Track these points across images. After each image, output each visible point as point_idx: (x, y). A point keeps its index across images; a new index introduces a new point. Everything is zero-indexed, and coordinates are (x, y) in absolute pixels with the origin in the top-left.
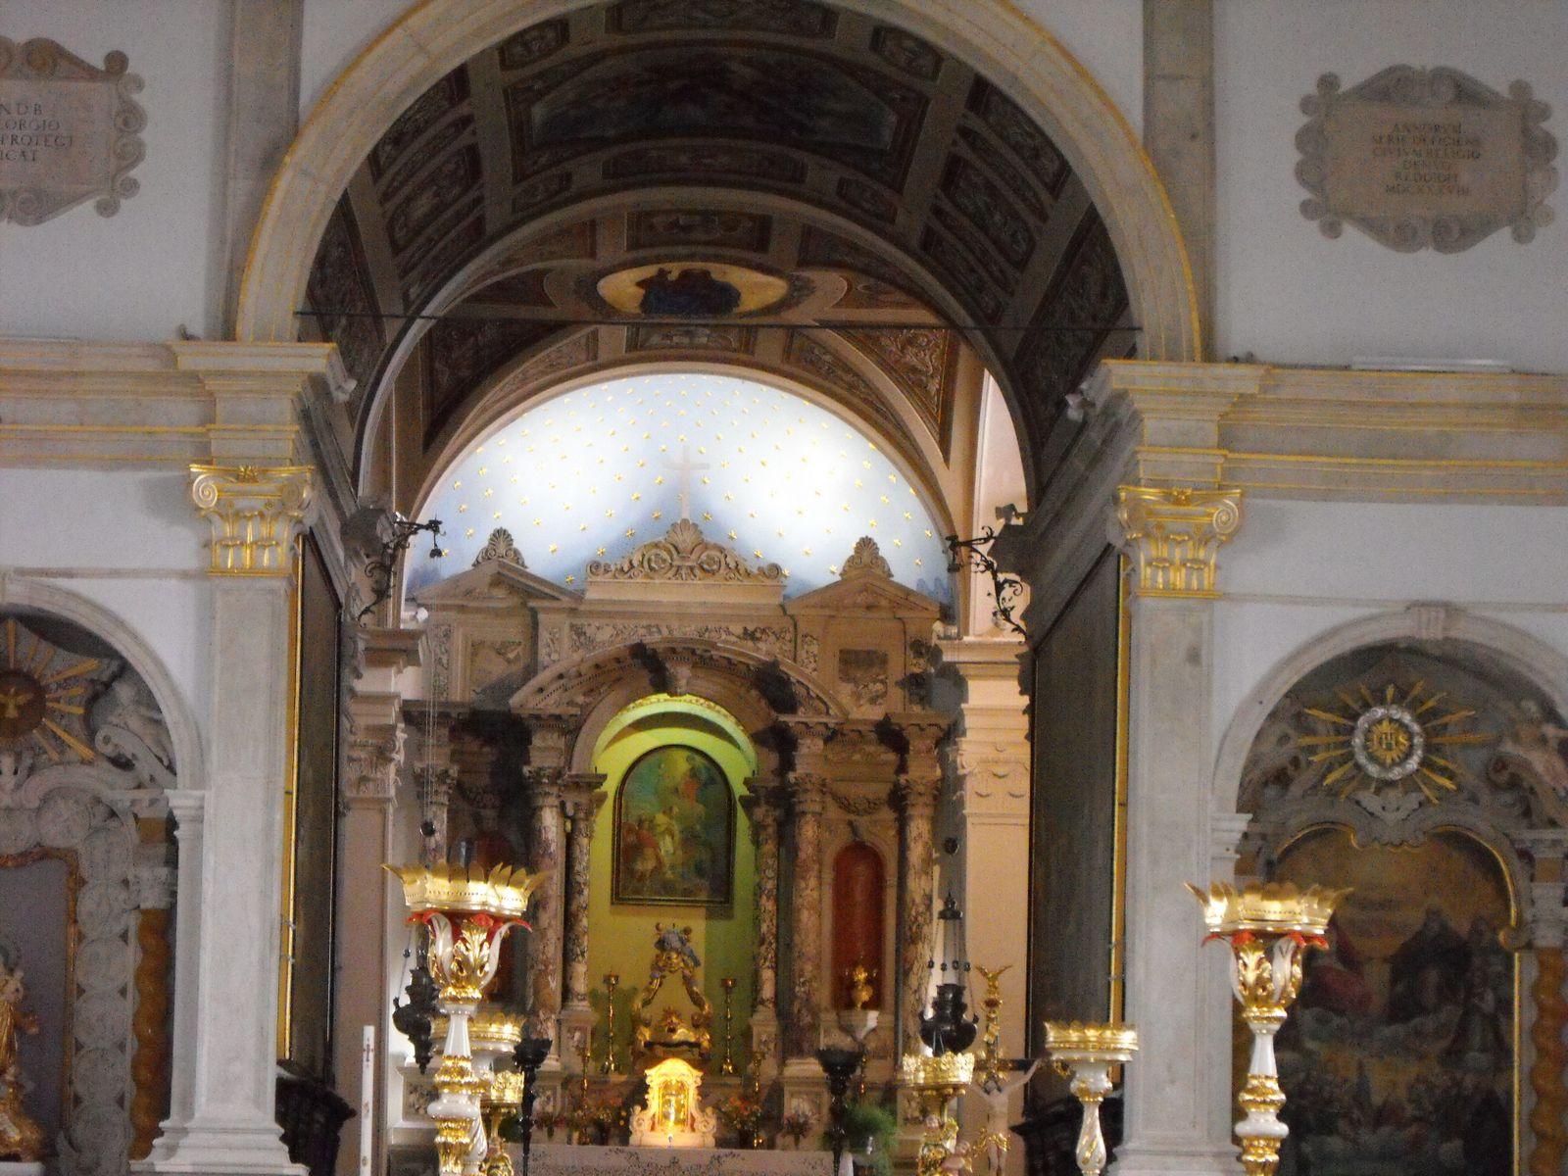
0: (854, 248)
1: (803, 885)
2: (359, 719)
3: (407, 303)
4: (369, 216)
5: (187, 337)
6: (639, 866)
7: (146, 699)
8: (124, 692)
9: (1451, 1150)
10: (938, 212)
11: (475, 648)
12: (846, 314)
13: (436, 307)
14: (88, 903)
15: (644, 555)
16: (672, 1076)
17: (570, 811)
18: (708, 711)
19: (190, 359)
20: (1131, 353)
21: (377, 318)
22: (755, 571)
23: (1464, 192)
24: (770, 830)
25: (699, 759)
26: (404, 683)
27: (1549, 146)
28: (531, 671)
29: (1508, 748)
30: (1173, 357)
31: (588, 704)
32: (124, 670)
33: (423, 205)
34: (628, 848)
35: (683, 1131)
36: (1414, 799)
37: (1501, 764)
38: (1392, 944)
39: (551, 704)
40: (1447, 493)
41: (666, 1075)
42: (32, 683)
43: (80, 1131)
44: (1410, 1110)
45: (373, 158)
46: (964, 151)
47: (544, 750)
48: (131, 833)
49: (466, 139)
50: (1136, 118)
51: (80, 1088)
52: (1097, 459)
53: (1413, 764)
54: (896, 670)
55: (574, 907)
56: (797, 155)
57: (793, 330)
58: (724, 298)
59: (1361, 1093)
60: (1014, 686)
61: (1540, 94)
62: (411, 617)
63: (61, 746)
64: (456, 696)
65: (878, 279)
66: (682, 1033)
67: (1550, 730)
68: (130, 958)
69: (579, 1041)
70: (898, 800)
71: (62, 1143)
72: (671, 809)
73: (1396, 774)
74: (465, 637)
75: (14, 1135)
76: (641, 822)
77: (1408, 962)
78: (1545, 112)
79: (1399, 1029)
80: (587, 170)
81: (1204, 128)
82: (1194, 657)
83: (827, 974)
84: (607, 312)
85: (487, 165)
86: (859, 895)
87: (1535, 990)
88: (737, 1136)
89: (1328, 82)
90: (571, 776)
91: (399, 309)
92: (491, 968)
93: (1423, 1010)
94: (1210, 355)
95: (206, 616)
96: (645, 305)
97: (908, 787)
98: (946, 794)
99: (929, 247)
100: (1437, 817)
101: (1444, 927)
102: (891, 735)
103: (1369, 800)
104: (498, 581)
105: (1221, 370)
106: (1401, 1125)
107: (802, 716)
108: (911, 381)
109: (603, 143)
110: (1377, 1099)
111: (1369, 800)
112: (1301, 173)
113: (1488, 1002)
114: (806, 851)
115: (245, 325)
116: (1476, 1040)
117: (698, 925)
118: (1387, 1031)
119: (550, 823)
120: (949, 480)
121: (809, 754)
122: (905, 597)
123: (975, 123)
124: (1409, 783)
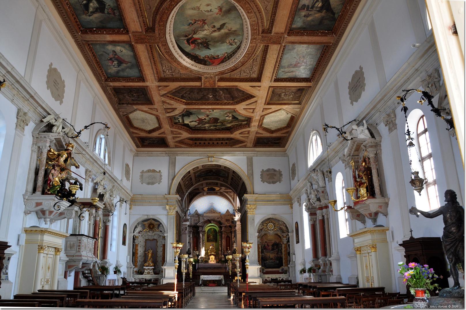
0: (225, 185)
2: (183, 227)
3: (186, 191)
4: (182, 183)
5: (166, 195)
7: (163, 226)
8: (161, 225)
9: (278, 262)
10: (231, 182)
11: (194, 220)
12: (225, 190)
13: (189, 191)
14: (158, 243)
16: (212, 257)
19: (166, 196)
20: (247, 194)
21: (184, 192)
23: (275, 179)
26: (188, 223)
27: (282, 175)
28: (199, 222)
29: (281, 226)
30: (250, 194)
32: (161, 223)
33: (187, 183)
34: (208, 237)
36: (273, 231)
37: (280, 228)
38: (272, 244)
39: (201, 225)
40: (275, 205)
42: (153, 224)
43: (157, 264)
44: (274, 258)
45: (182, 178)
46: (233, 177)
47: (200, 229)
48: (162, 237)
49: (190, 177)
50: (247, 174)
51: (157, 260)
52: (245, 203)
53: (273, 228)
54: (231, 221)
56: (219, 177)
57: (220, 192)
58: (214, 190)
59: (269, 257)
60: (239, 222)
61: (281, 170)
62: (189, 218)
63: (156, 230)
64: (193, 224)
65: (228, 188)
66: (213, 253)
67: (284, 225)
68: (162, 248)
70: (231, 232)
71: (156, 265)
73: (271, 229)
75: (151, 264)
77: (273, 245)
78: (281, 172)
79: (273, 251)
80: (201, 179)
81: (252, 175)
82: (253, 220)
83: (225, 248)
84: (205, 191)
85: (192, 179)
86: (228, 240)
87: (284, 247)
88: (217, 262)
89: (263, 170)
91: (185, 191)
92: (179, 252)
93: (274, 250)
94: (254, 194)
95: (168, 218)
96: (208, 190)
98: (235, 231)
99: (231, 185)
100: (275, 233)
101: (276, 242)
102: (230, 226)
103: (269, 231)
104: (196, 214)
105: (255, 195)
106: (273, 260)
107: (223, 225)
108: (231, 196)
109: (203, 177)
110: (271, 257)
111: (269, 231)
112: (261, 178)
113: (280, 248)
114: (223, 237)
115: (171, 193)
116: (279, 252)
117: (214, 244)
118: (271, 252)
119: (201, 235)
120: (234, 204)
121: (223, 229)
122: (231, 215)
123: (233, 174)
124: (273, 230)
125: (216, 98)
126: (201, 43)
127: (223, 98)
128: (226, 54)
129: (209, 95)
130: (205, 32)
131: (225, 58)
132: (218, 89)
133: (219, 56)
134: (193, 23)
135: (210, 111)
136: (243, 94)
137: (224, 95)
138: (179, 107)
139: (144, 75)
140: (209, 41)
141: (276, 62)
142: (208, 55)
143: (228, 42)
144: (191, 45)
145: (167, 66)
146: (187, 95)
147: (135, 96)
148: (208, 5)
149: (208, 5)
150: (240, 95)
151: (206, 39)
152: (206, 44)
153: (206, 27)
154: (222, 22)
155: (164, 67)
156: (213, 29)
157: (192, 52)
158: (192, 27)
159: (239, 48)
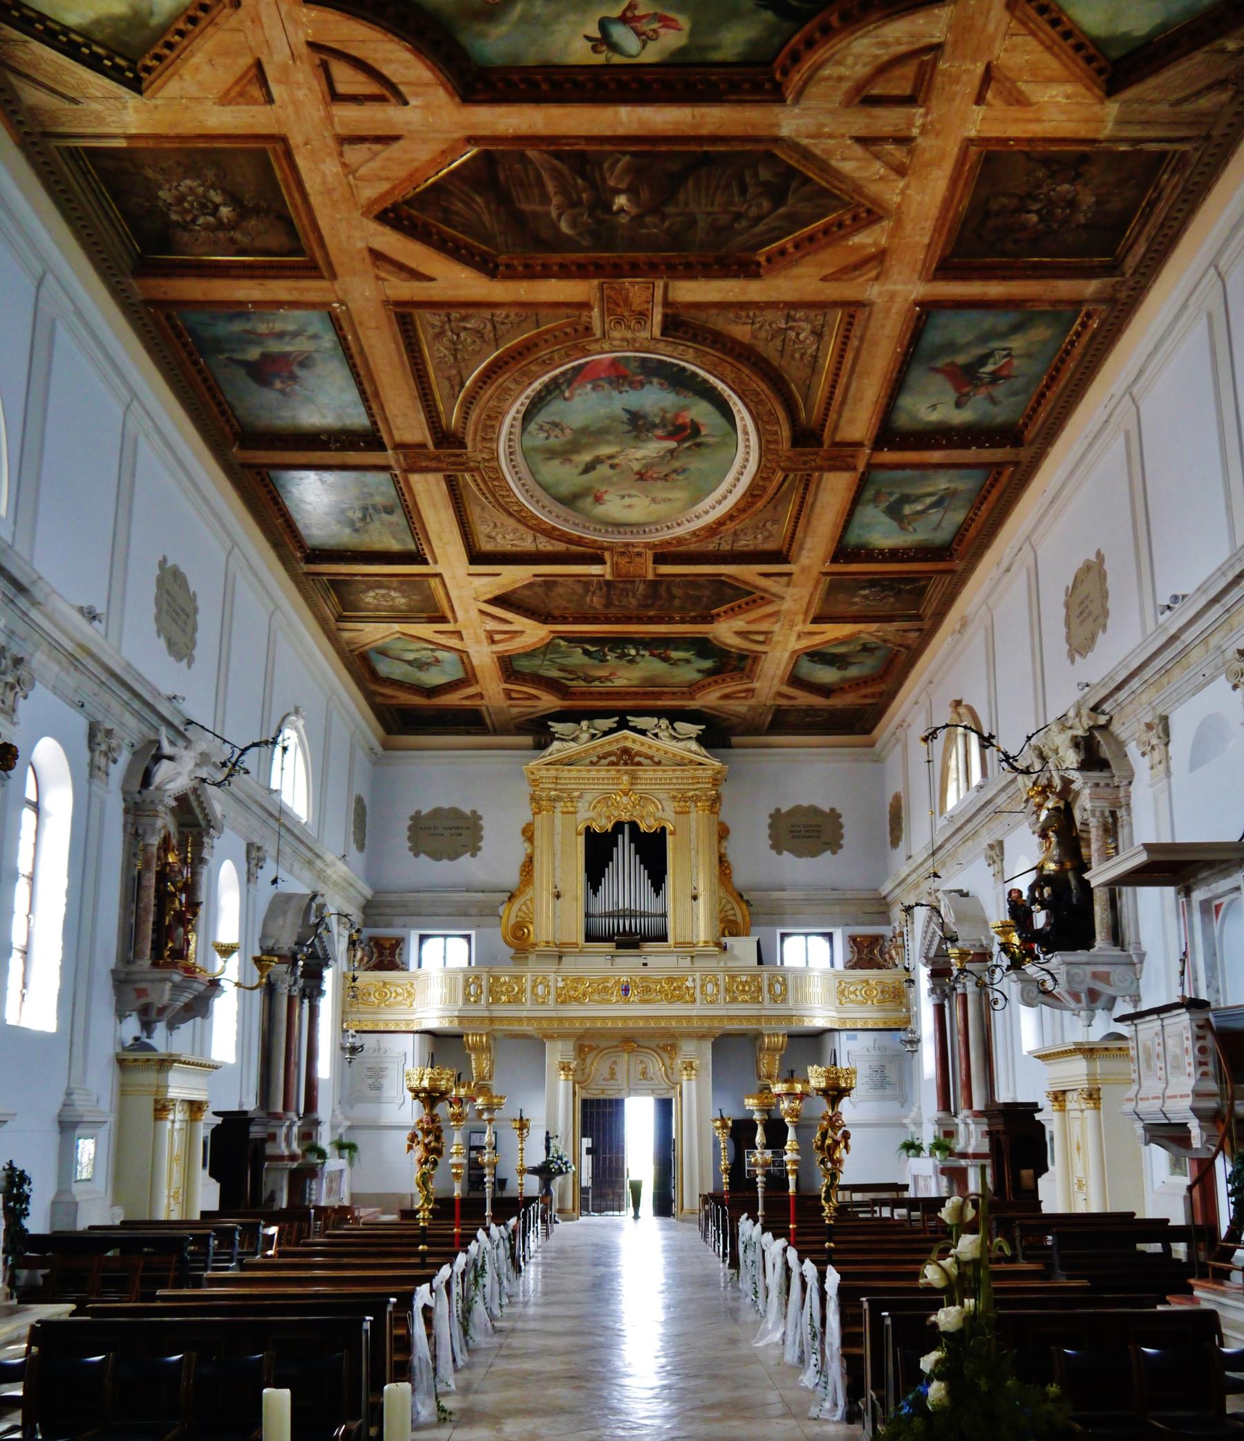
125: (593, 186)
126: (655, 426)
127: (550, 187)
128: (567, 394)
129: (634, 211)
130: (639, 454)
131: (570, 384)
132: (584, 243)
133: (594, 389)
134: (674, 476)
135: (623, 19)
136: (446, 211)
137: (548, 214)
138: (832, 112)
139: (905, 342)
140: (628, 432)
141: (377, 394)
142: (631, 392)
143: (568, 432)
144: (688, 420)
145: (797, 355)
146: (753, 212)
147: (1037, 212)
148: (630, 506)
149: (630, 506)
150: (459, 206)
151: (637, 438)
152: (638, 424)
153: (636, 466)
154: (592, 476)
155: (809, 351)
156: (616, 461)
157: (687, 401)
158: (677, 464)
159: (528, 416)
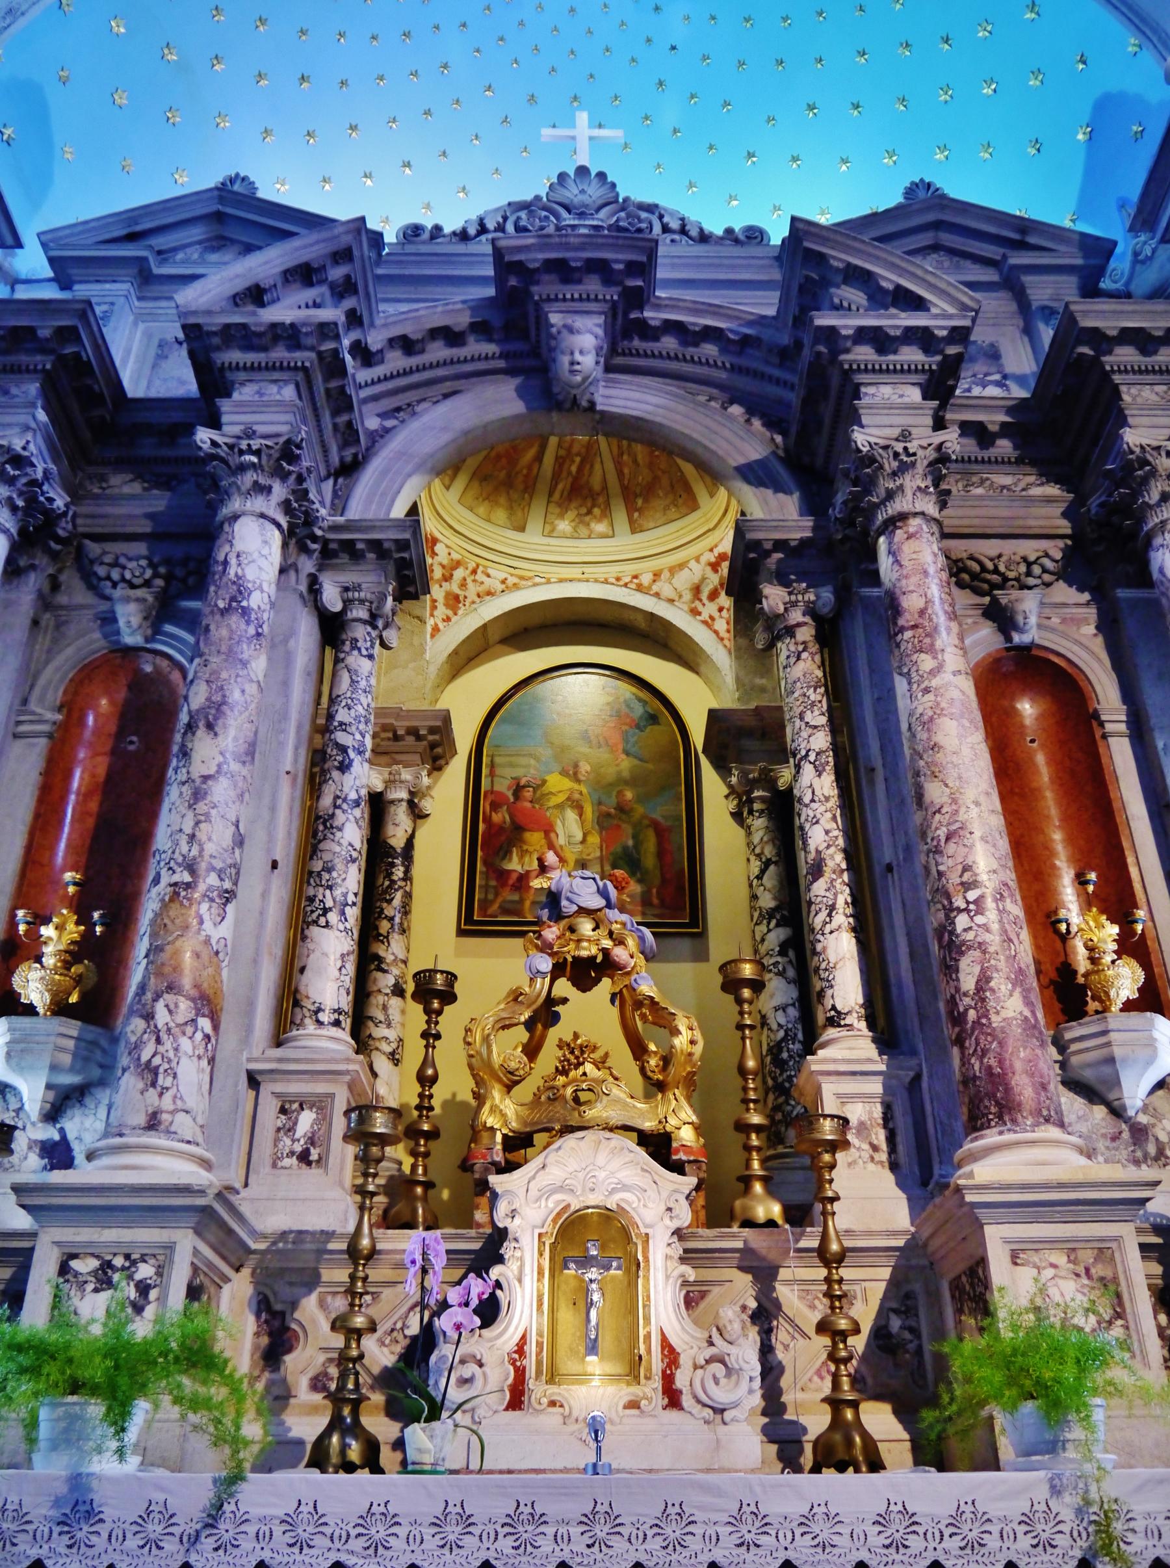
1: (926, 662)
6: (514, 865)
15: (505, 218)
17: (332, 598)
18: (639, 595)
22: (719, 231)
24: (806, 634)
25: (626, 690)
31: (387, 431)
35: (633, 1405)
41: (561, 1189)
55: (326, 801)
69: (312, 1141)
72: (576, 766)
74: (148, 335)
76: (518, 789)
90: (335, 528)
97: (1144, 462)
